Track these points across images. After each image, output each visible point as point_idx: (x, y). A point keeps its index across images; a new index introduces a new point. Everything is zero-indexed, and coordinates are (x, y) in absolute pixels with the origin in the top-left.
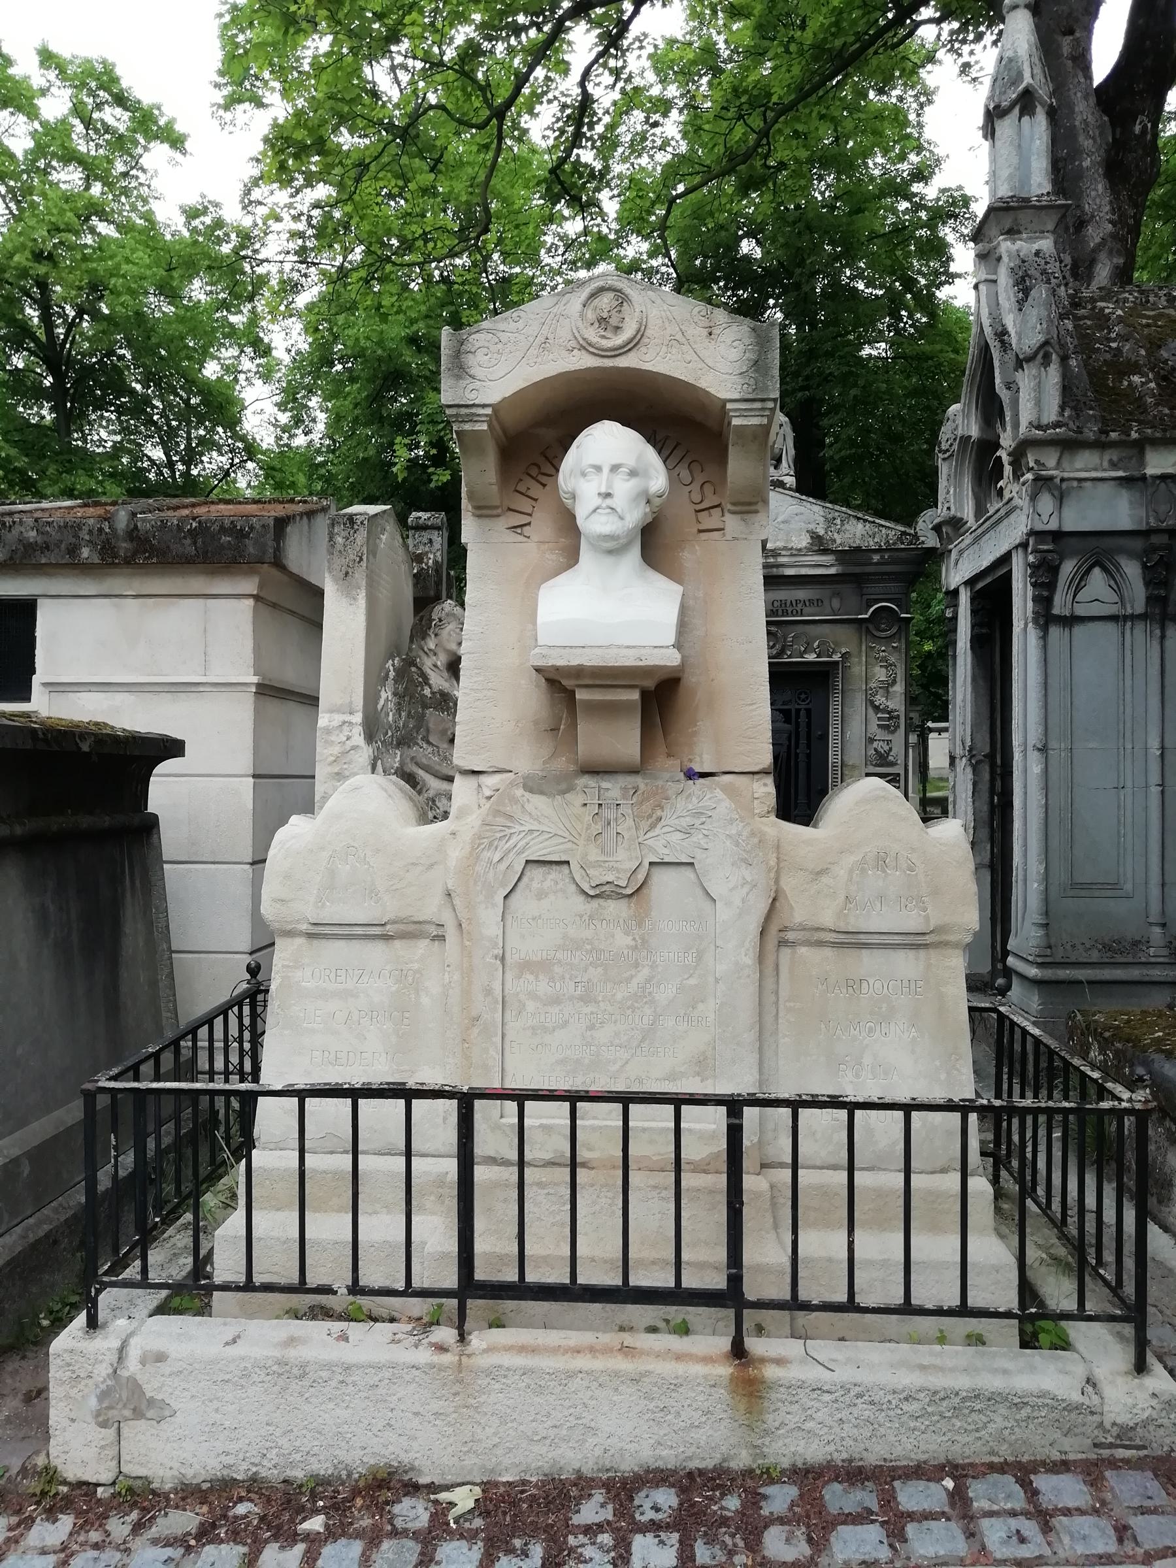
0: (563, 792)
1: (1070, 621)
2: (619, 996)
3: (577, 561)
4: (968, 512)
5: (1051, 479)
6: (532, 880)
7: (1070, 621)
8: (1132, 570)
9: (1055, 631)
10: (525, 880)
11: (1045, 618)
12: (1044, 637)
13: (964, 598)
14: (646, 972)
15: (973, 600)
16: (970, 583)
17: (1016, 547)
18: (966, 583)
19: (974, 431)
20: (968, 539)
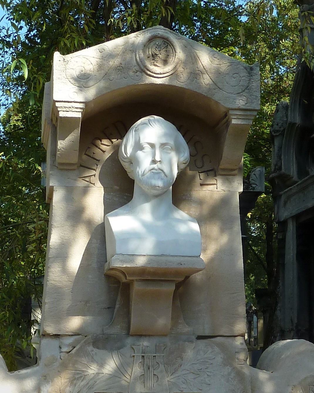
0: (119, 348)
3: (132, 197)
4: (293, 171)
13: (291, 228)
16: (296, 217)
18: (293, 217)
20: (294, 189)
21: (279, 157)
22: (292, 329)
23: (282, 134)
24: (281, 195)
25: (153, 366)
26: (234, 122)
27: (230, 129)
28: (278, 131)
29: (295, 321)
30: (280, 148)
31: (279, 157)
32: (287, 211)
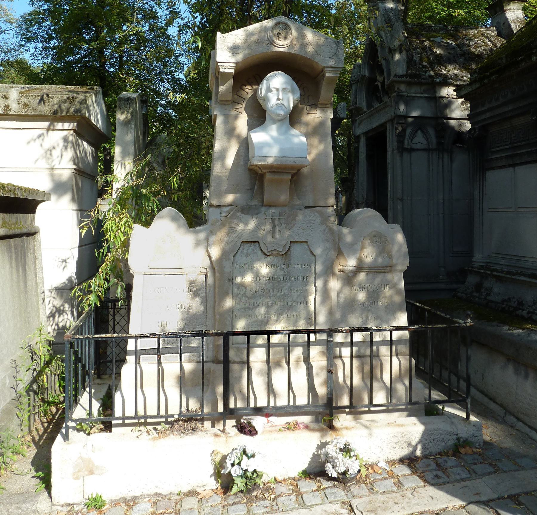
0: (257, 214)
1: (411, 150)
2: (278, 294)
4: (364, 105)
5: (403, 96)
6: (243, 249)
7: (411, 150)
8: (431, 132)
9: (405, 155)
10: (241, 249)
11: (402, 149)
12: (401, 156)
13: (363, 140)
14: (289, 284)
15: (367, 140)
16: (366, 133)
17: (389, 121)
18: (364, 133)
19: (367, 74)
20: (364, 116)
21: (355, 96)
22: (363, 202)
23: (357, 82)
24: (356, 120)
25: (278, 225)
26: (327, 75)
27: (325, 79)
28: (354, 81)
29: (365, 197)
30: (356, 91)
31: (355, 96)
32: (360, 130)
